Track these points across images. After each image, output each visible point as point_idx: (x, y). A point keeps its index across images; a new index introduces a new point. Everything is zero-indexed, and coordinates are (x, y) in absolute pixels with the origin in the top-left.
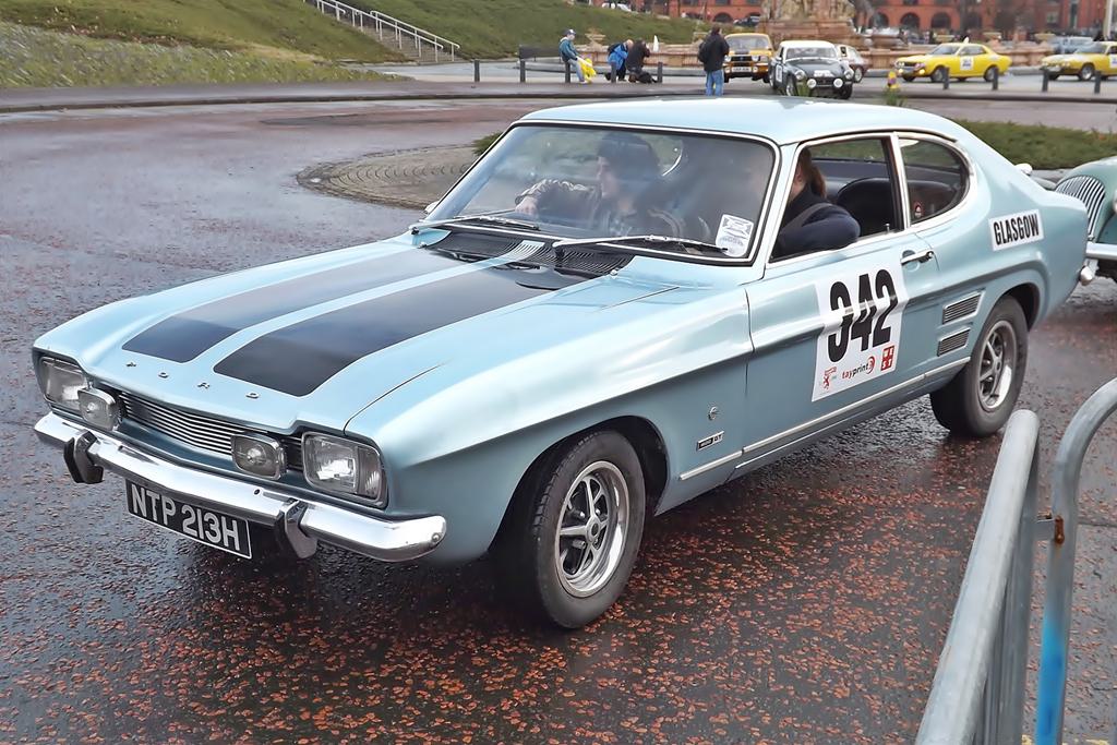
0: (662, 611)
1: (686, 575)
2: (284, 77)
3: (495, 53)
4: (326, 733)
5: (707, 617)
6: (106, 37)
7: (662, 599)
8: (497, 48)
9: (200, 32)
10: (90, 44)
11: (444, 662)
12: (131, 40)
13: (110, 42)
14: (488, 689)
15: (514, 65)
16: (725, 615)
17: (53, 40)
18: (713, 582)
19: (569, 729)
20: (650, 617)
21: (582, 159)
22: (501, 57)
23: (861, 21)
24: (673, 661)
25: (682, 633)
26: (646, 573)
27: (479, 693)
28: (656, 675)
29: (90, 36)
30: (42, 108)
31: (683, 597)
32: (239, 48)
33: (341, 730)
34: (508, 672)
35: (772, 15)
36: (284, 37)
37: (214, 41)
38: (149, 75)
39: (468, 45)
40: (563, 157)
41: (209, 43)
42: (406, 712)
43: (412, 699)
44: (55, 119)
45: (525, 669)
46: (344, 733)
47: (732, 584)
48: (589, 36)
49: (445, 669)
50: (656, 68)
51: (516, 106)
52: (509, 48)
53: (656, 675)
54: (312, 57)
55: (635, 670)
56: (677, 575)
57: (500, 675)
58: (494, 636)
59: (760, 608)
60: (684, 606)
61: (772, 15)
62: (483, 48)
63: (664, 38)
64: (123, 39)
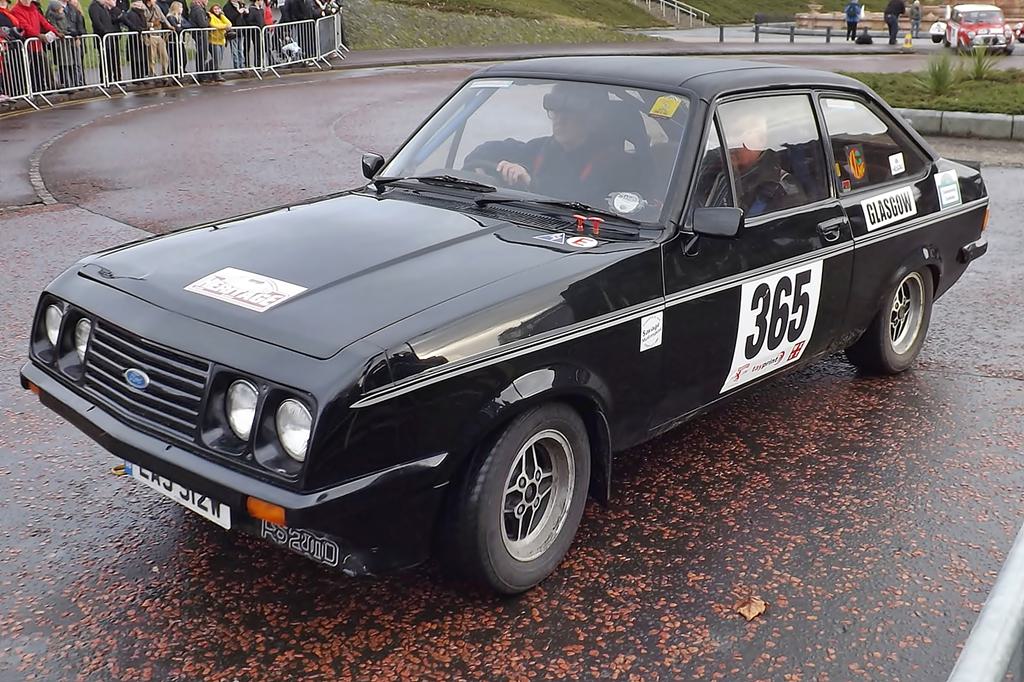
0: (845, 450)
1: (867, 425)
2: (577, 40)
3: (736, 19)
4: (595, 521)
5: (881, 457)
6: (451, 11)
7: (846, 441)
8: (738, 16)
9: (517, 6)
10: (444, 17)
11: (681, 478)
12: (468, 13)
13: (453, 14)
14: (712, 499)
15: (751, 28)
16: (895, 456)
17: (414, 13)
18: (887, 430)
19: (771, 532)
20: (836, 454)
24: (853, 488)
25: (861, 469)
26: (836, 421)
27: (706, 501)
28: (839, 497)
29: (440, 10)
30: (405, 64)
31: (863, 441)
32: (545, 17)
33: (605, 520)
34: (726, 487)
36: (577, 10)
37: (527, 12)
38: (480, 38)
39: (715, 14)
41: (523, 15)
42: (652, 511)
43: (656, 502)
44: (414, 72)
45: (740, 486)
46: (607, 522)
47: (901, 433)
48: (810, 6)
49: (681, 483)
52: (748, 16)
53: (839, 497)
54: (598, 24)
55: (823, 492)
56: (860, 424)
57: (722, 490)
58: (718, 461)
59: (924, 453)
60: (864, 447)
62: (726, 15)
64: (462, 12)
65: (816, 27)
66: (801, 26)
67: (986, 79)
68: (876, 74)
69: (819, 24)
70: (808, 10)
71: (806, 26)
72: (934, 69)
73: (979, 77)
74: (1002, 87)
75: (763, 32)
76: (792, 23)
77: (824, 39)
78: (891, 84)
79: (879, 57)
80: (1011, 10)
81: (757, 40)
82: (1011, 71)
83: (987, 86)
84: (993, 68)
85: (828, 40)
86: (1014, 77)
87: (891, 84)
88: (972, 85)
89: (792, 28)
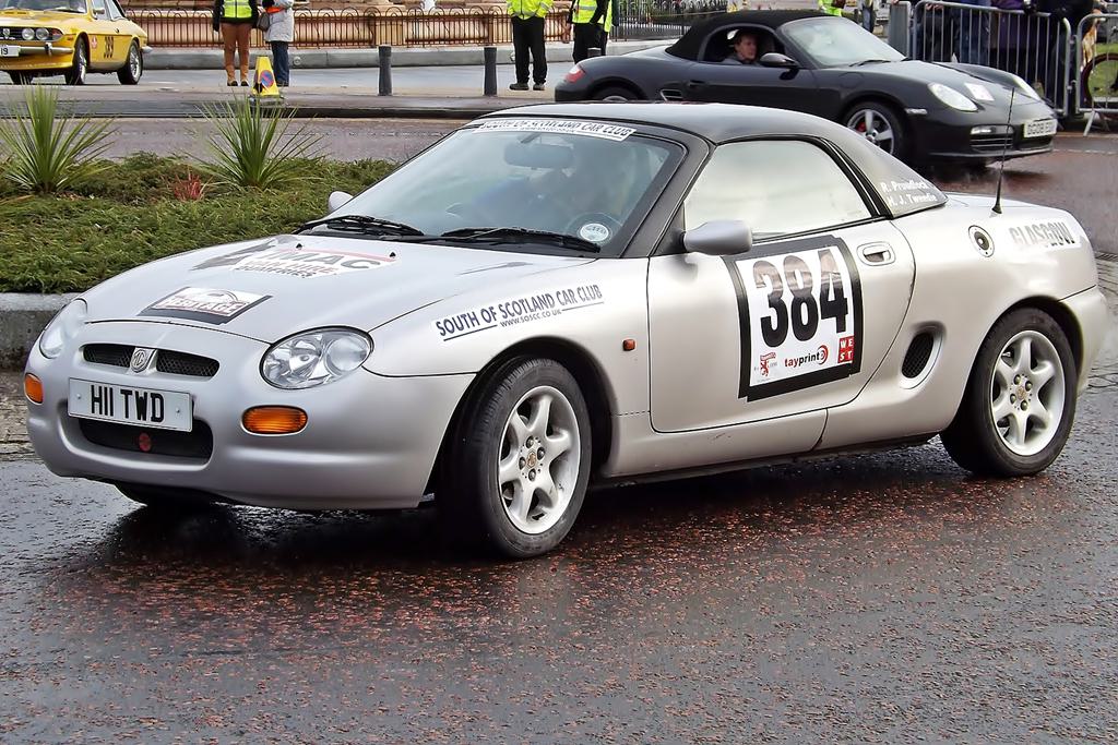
67: (67, 189)
73: (44, 187)
74: (113, 211)
82: (142, 163)
83: (69, 213)
84: (80, 159)
86: (150, 182)
88: (24, 209)
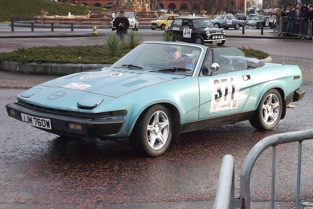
15: (9, 24)
21: (40, 62)
22: (3, 21)
23: (153, 6)
35: (117, 4)
40: (31, 61)
50: (70, 25)
51: (10, 41)
61: (117, 4)
63: (73, 13)
65: (45, 23)
66: (37, 23)
68: (80, 47)
69: (47, 21)
70: (40, 14)
71: (40, 23)
72: (110, 44)
75: (17, 26)
76: (33, 21)
77: (50, 30)
78: (88, 51)
79: (80, 38)
80: (145, 14)
81: (13, 30)
85: (52, 30)
87: (88, 51)
89: (32, 23)
